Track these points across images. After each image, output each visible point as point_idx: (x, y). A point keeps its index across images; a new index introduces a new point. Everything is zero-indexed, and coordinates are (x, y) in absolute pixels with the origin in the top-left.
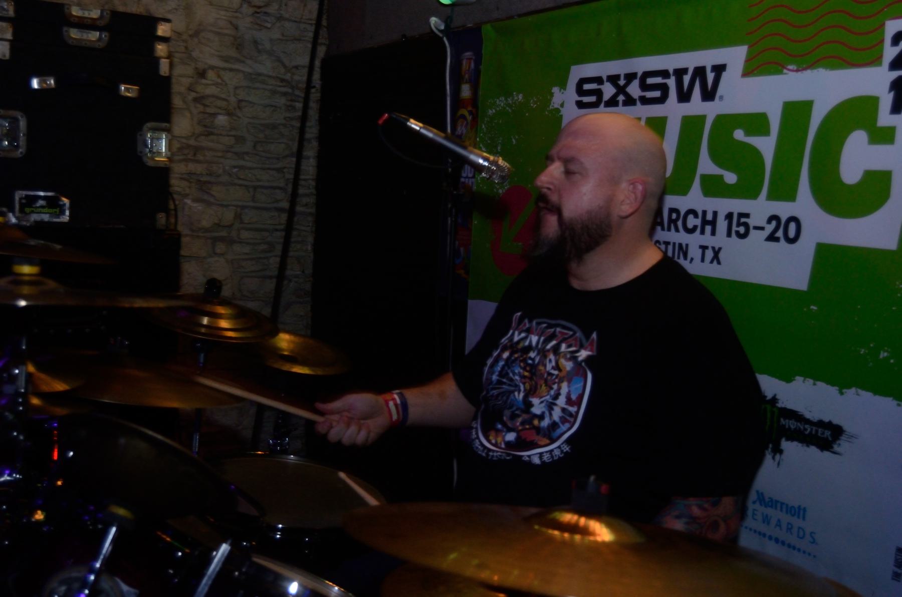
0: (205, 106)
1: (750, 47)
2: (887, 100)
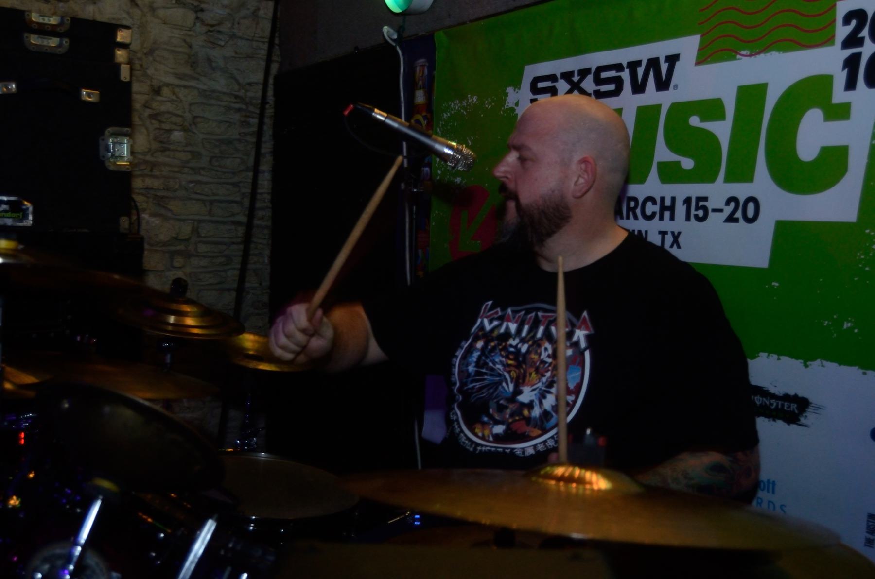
0: (161, 122)
1: (702, 36)
2: (840, 77)
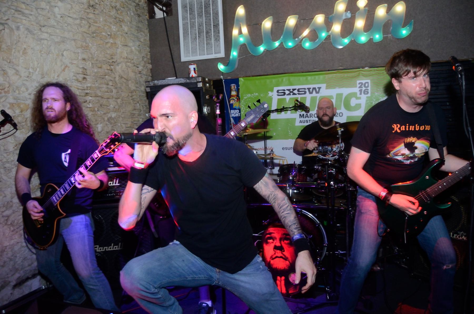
2: (359, 93)
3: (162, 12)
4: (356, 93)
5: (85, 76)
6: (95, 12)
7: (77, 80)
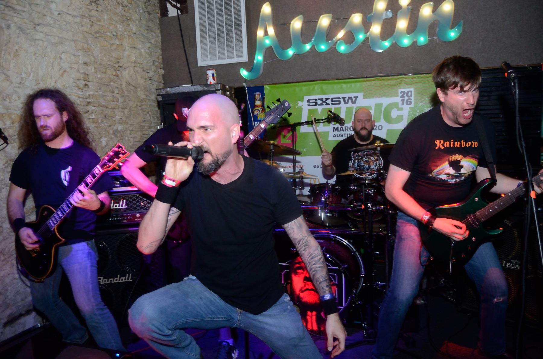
2: (400, 103)
3: (176, 9)
4: (397, 103)
5: (87, 83)
6: (98, 9)
7: (78, 87)
